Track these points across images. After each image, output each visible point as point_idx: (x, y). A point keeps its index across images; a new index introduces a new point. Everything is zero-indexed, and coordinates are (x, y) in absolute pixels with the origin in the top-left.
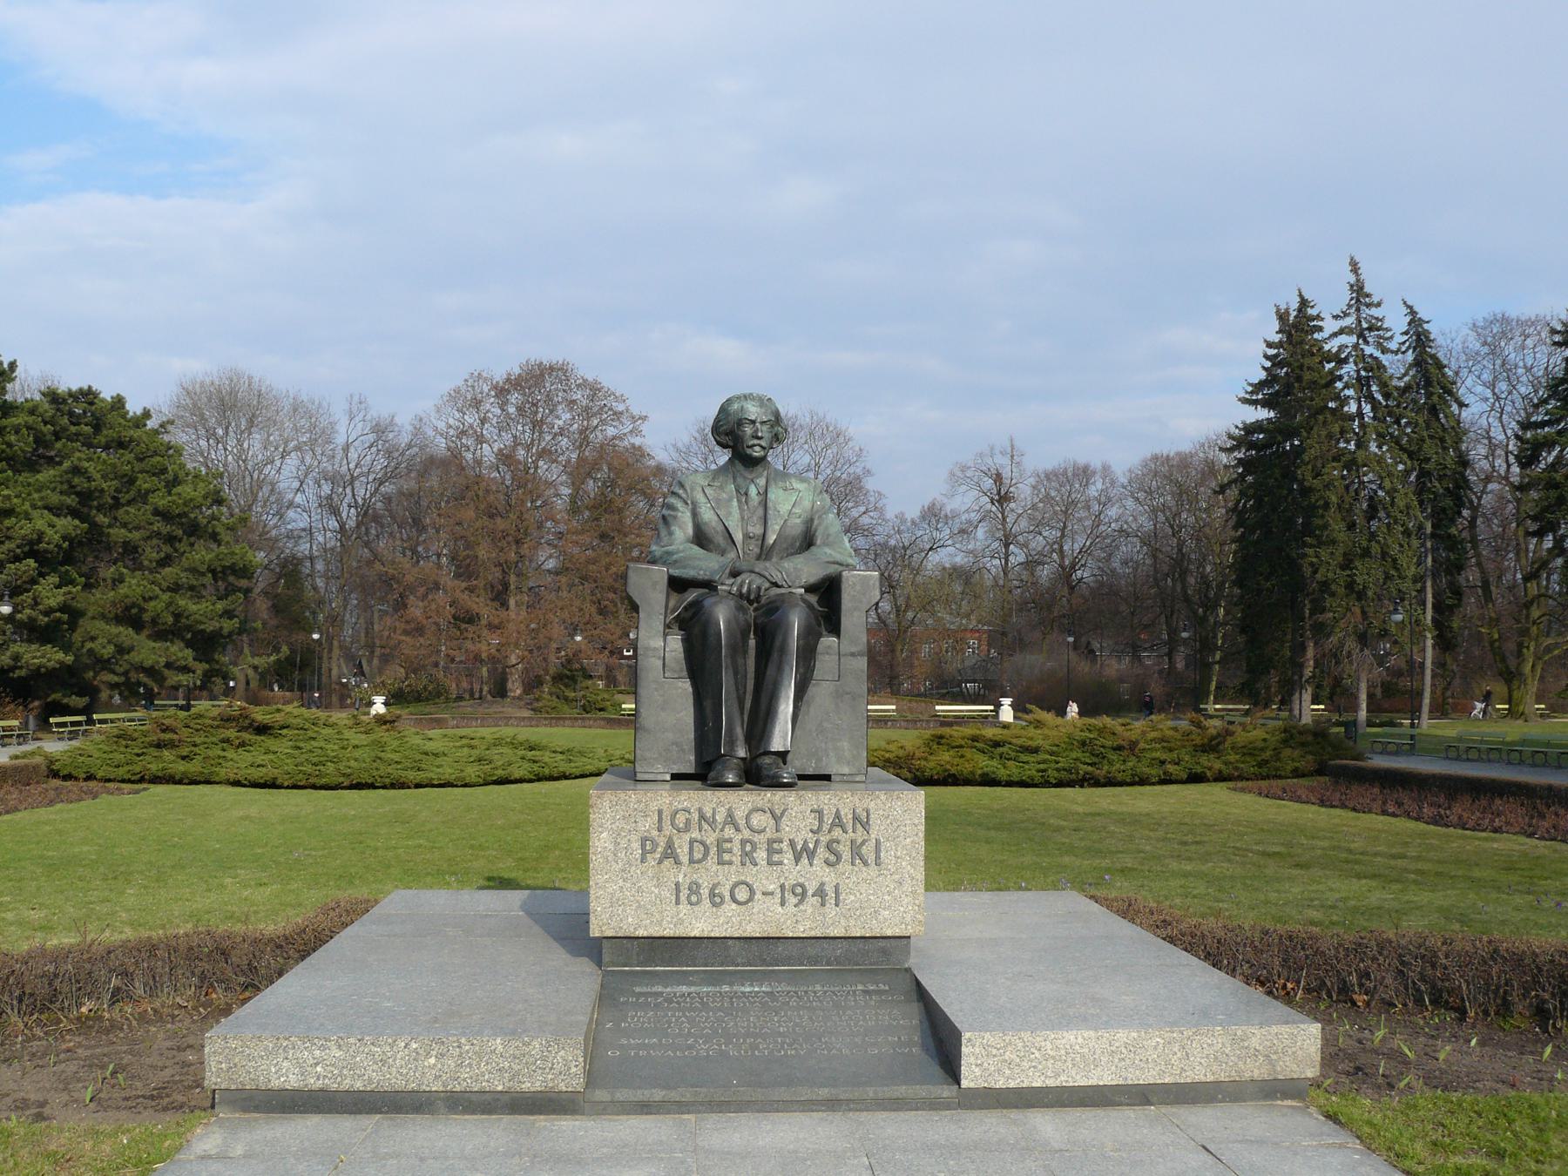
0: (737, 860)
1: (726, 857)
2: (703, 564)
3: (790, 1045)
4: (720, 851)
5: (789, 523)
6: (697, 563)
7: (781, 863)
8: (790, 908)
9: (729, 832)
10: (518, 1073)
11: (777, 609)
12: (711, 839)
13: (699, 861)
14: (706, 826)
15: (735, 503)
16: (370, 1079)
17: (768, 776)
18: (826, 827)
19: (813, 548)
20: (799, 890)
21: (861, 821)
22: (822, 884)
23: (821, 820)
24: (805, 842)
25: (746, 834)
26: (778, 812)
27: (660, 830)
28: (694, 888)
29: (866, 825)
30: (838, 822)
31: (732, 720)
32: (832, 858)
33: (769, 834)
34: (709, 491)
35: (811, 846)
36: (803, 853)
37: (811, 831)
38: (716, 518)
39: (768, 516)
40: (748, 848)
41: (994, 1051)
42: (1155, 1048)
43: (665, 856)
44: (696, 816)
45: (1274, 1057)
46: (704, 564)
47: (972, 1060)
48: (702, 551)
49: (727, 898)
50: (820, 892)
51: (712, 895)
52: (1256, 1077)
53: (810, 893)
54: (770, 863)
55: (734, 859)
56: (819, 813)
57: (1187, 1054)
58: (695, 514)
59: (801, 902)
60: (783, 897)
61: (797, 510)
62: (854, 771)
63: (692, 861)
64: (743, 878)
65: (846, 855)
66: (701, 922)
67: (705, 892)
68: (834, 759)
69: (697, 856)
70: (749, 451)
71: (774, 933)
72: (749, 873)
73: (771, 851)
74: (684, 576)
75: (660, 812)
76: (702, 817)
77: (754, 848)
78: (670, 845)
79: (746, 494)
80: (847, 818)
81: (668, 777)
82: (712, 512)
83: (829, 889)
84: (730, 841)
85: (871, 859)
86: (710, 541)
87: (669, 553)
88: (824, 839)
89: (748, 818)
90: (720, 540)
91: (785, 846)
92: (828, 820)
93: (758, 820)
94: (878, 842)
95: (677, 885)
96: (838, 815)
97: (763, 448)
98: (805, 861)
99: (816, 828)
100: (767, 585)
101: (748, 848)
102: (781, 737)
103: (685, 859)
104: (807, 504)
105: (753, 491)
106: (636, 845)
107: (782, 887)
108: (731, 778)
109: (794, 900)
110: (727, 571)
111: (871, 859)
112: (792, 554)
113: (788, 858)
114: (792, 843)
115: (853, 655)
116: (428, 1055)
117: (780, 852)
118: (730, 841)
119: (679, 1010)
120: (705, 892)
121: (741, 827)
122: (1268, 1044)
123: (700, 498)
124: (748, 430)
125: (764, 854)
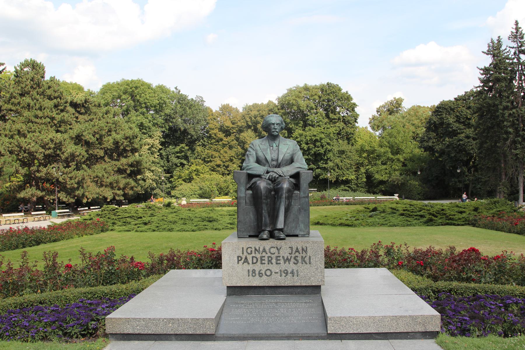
0: (266, 262)
1: (263, 262)
3: (279, 320)
4: (262, 260)
5: (286, 156)
6: (256, 169)
7: (280, 263)
8: (283, 277)
9: (264, 254)
10: (196, 328)
11: (280, 184)
12: (258, 256)
13: (255, 263)
14: (257, 252)
15: (269, 150)
16: (153, 330)
18: (294, 252)
20: (286, 272)
21: (305, 250)
22: (293, 270)
23: (292, 250)
24: (288, 257)
25: (269, 255)
26: (279, 248)
27: (243, 254)
28: (254, 271)
29: (306, 252)
30: (297, 251)
31: (266, 218)
32: (296, 262)
33: (276, 254)
34: (260, 145)
35: (289, 258)
36: (288, 260)
37: (289, 253)
40: (270, 259)
41: (338, 322)
42: (388, 321)
43: (244, 262)
44: (254, 249)
45: (426, 325)
46: (259, 169)
47: (331, 325)
49: (264, 274)
50: (292, 273)
51: (259, 273)
52: (420, 331)
53: (289, 272)
54: (277, 264)
55: (266, 262)
56: (291, 248)
57: (398, 323)
58: (256, 154)
59: (287, 275)
60: (281, 274)
61: (288, 151)
62: (305, 233)
63: (253, 263)
64: (268, 268)
65: (300, 261)
66: (257, 282)
67: (257, 272)
69: (255, 261)
70: (273, 133)
71: (278, 285)
72: (270, 267)
73: (277, 260)
75: (243, 248)
76: (256, 249)
77: (272, 259)
78: (246, 258)
79: (272, 146)
80: (300, 250)
81: (248, 236)
83: (295, 271)
84: (264, 257)
85: (308, 262)
87: (248, 166)
88: (293, 256)
89: (270, 249)
90: (264, 161)
91: (281, 258)
92: (294, 250)
93: (273, 250)
94: (310, 257)
95: (249, 271)
96: (297, 249)
97: (277, 132)
98: (287, 263)
99: (290, 252)
101: (270, 259)
102: (280, 224)
103: (251, 262)
104: (292, 149)
105: (274, 145)
106: (236, 259)
107: (281, 271)
108: (265, 236)
109: (284, 275)
111: (308, 262)
113: (282, 262)
114: (283, 257)
115: (304, 197)
116: (169, 323)
117: (280, 260)
118: (264, 257)
119: (248, 309)
120: (257, 272)
121: (268, 253)
122: (424, 320)
123: (258, 148)
124: (273, 126)
125: (275, 261)
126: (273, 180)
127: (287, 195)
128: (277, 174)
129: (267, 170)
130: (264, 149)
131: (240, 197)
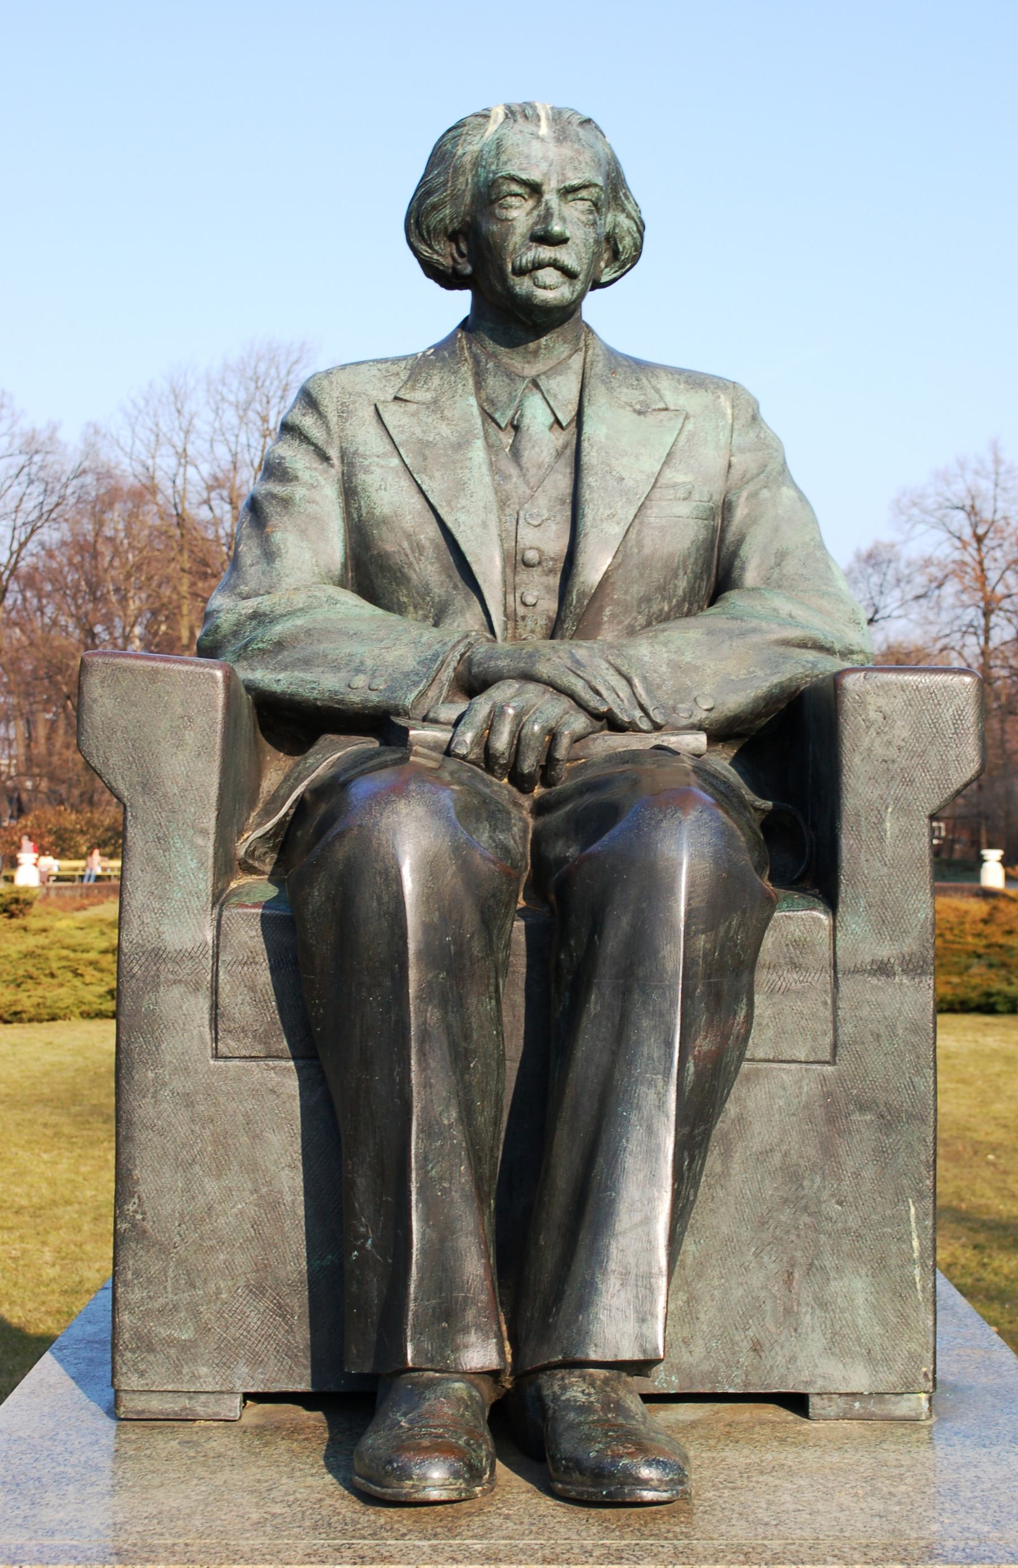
2: (363, 651)
5: (654, 516)
6: (347, 648)
15: (478, 452)
17: (577, 1465)
19: (733, 598)
34: (392, 415)
38: (416, 502)
39: (586, 494)
48: (368, 609)
58: (349, 492)
62: (888, 1379)
68: (816, 1341)
70: (523, 286)
74: (306, 692)
82: (405, 483)
86: (398, 576)
97: (569, 274)
100: (580, 722)
110: (447, 674)
112: (664, 618)
115: (883, 969)
126: (529, 764)
127: (702, 942)
128: (581, 705)
129: (466, 661)
130: (423, 447)
131: (157, 955)
